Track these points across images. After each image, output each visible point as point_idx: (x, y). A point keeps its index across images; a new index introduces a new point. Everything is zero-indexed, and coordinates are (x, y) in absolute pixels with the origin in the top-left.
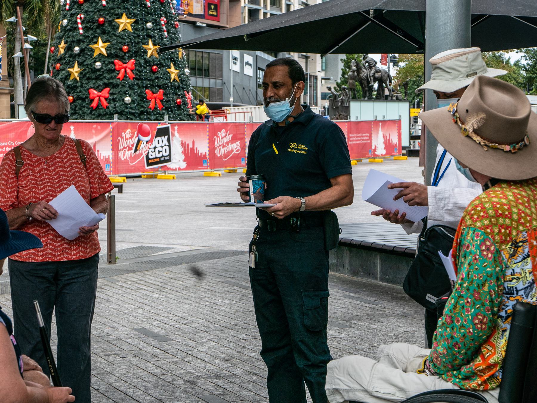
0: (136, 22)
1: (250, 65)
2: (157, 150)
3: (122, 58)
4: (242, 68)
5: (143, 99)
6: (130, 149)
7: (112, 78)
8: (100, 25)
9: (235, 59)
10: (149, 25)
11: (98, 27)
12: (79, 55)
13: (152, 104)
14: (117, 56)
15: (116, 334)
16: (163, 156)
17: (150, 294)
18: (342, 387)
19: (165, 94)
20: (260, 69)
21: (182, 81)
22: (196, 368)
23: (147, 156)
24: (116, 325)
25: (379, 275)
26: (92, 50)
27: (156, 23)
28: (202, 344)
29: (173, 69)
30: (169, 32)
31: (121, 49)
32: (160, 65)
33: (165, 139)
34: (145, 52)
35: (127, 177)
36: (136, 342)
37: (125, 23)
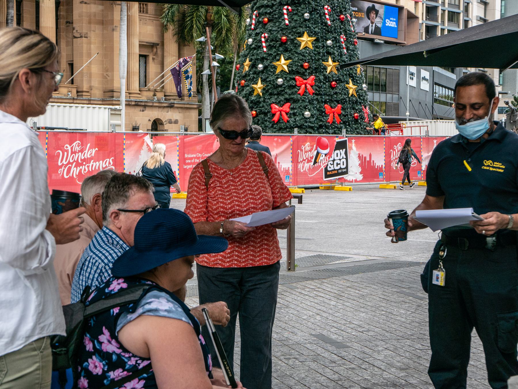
0: (317, 40)
1: (427, 80)
2: (335, 162)
3: (303, 75)
4: (419, 83)
5: (322, 113)
6: (309, 161)
7: (293, 93)
8: (283, 43)
9: (412, 74)
10: (329, 42)
11: (280, 45)
12: (262, 72)
13: (330, 118)
14: (298, 73)
15: (295, 338)
16: (341, 169)
17: (328, 301)
19: (343, 109)
20: (436, 84)
21: (359, 96)
22: (373, 375)
23: (326, 169)
24: (295, 330)
26: (275, 67)
27: (336, 40)
28: (379, 352)
29: (351, 85)
30: (348, 49)
31: (302, 66)
32: (339, 81)
33: (343, 152)
34: (325, 68)
35: (306, 188)
36: (314, 347)
37: (306, 41)
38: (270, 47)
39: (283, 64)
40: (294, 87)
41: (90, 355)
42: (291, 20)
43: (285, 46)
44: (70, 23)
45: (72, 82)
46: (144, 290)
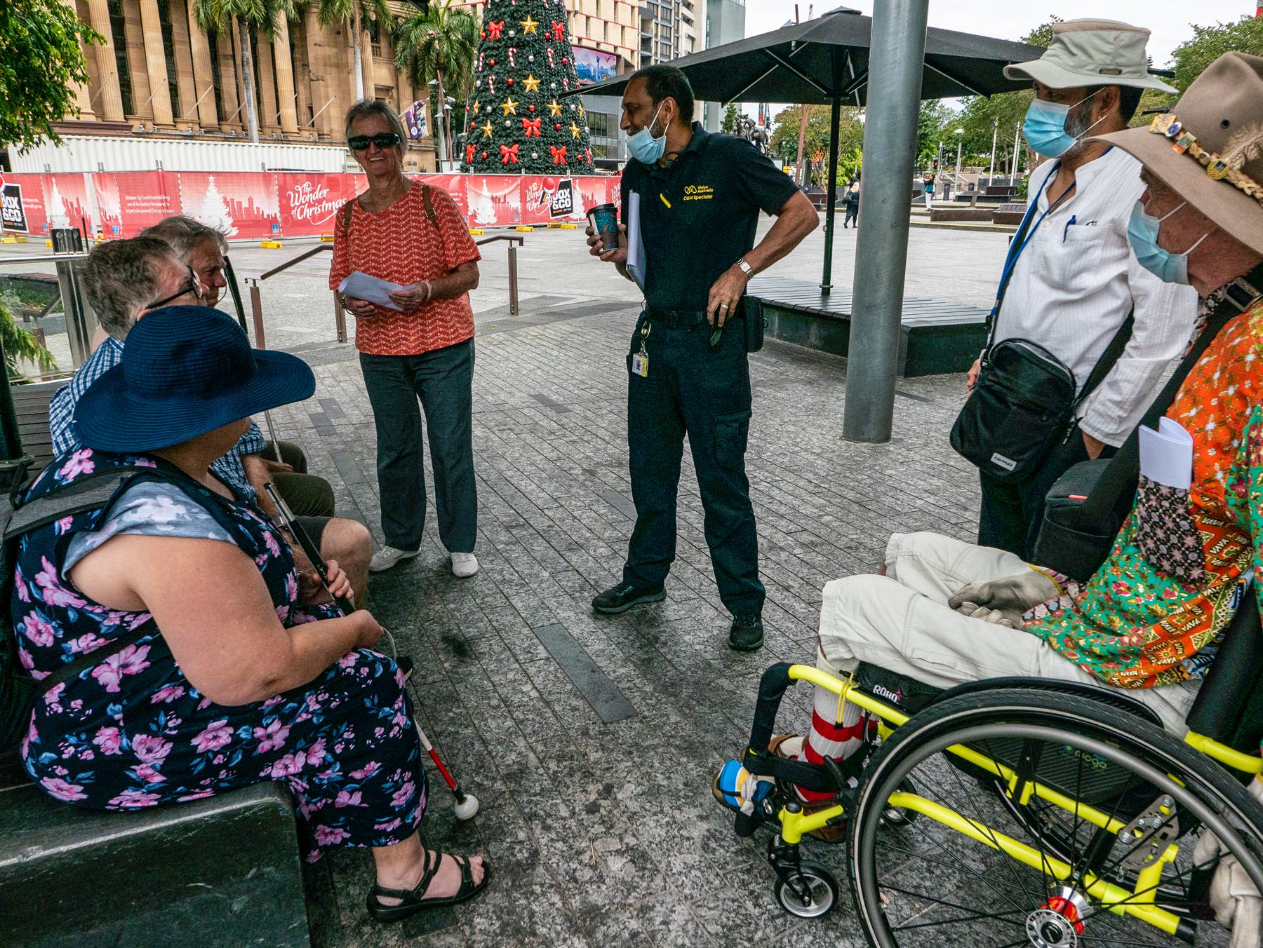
0: (542, 83)
3: (529, 117)
5: (548, 154)
8: (510, 86)
10: (553, 85)
13: (556, 160)
14: (525, 115)
15: (513, 401)
17: (549, 351)
18: (851, 636)
22: (596, 450)
24: (513, 390)
25: (776, 332)
26: (503, 110)
28: (602, 416)
34: (550, 111)
36: (533, 412)
37: (531, 83)
38: (497, 89)
39: (510, 106)
40: (519, 129)
41: (26, 609)
42: (516, 62)
43: (513, 89)
44: (306, 65)
45: (313, 125)
46: (122, 479)
